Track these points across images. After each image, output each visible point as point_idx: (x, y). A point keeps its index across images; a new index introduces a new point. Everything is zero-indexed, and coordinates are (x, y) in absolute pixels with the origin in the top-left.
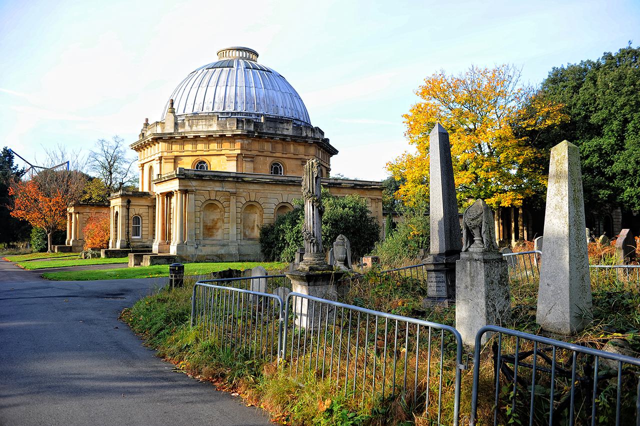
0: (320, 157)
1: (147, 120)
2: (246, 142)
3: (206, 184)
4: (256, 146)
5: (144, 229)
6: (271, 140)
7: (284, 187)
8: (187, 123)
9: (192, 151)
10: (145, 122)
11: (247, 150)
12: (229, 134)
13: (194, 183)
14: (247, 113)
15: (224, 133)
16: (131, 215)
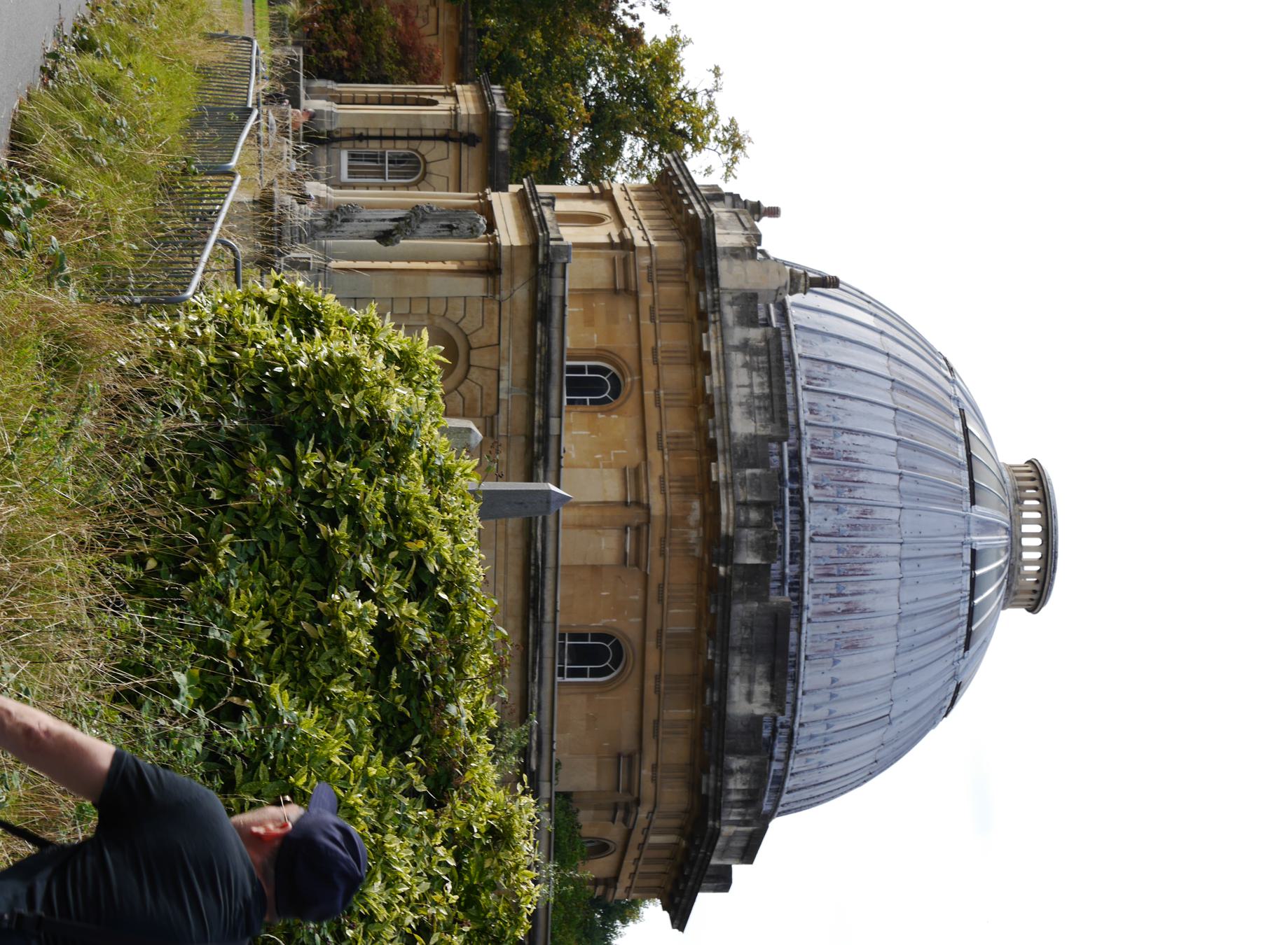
0: (654, 839)
1: (774, 212)
2: (694, 535)
3: (521, 334)
4: (681, 575)
6: (704, 629)
7: (517, 609)
8: (755, 334)
9: (655, 351)
11: (663, 540)
12: (720, 471)
13: (521, 294)
14: (802, 546)
15: (720, 458)
16: (424, 147)
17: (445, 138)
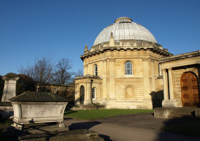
8: (121, 43)
16: (92, 88)
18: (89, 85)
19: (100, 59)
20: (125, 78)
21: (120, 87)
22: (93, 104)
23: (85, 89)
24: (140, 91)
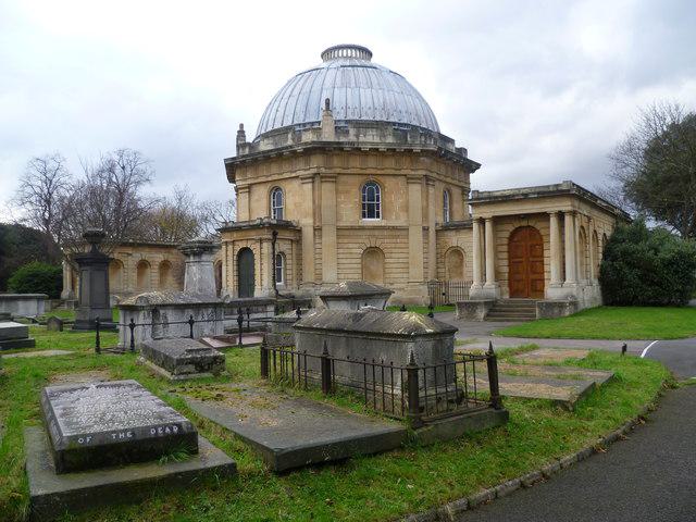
1: (242, 126)
5: (288, 272)
8: (352, 131)
10: (238, 129)
12: (417, 149)
17: (273, 244)
18: (267, 247)
19: (292, 172)
20: (362, 228)
21: (349, 251)
22: (282, 296)
23: (257, 257)
24: (401, 260)
